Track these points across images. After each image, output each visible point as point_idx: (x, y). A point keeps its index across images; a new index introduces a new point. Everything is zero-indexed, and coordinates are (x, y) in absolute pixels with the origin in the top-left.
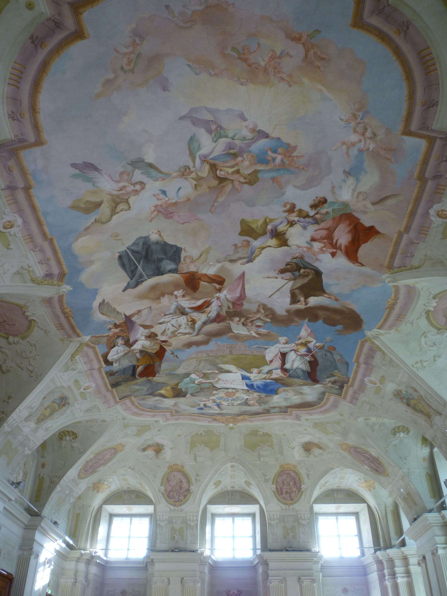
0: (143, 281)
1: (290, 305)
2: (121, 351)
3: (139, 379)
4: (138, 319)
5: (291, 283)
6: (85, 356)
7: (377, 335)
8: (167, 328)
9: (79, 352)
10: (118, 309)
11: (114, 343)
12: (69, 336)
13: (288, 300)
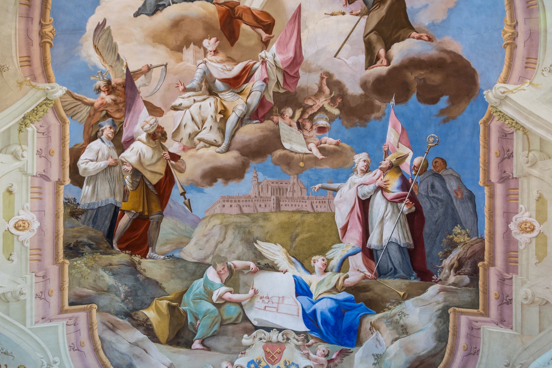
0: (164, 6)
1: (366, 69)
2: (103, 155)
3: (117, 253)
4: (145, 85)
5: (363, 21)
6: (43, 133)
7: (504, 93)
8: (184, 123)
9: (37, 117)
10: (122, 50)
11: (97, 130)
12: (34, 79)
13: (362, 58)
